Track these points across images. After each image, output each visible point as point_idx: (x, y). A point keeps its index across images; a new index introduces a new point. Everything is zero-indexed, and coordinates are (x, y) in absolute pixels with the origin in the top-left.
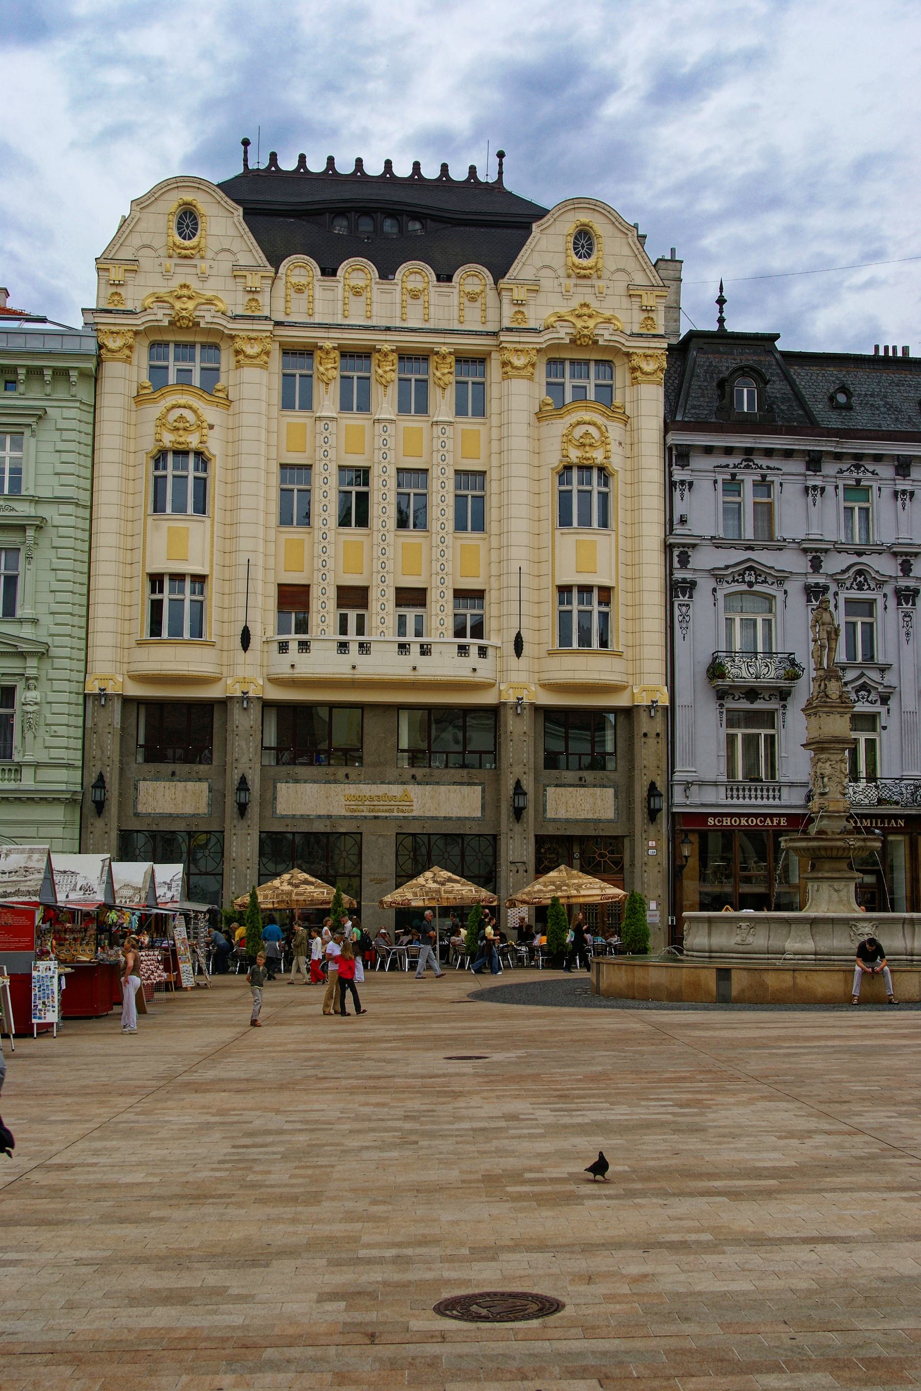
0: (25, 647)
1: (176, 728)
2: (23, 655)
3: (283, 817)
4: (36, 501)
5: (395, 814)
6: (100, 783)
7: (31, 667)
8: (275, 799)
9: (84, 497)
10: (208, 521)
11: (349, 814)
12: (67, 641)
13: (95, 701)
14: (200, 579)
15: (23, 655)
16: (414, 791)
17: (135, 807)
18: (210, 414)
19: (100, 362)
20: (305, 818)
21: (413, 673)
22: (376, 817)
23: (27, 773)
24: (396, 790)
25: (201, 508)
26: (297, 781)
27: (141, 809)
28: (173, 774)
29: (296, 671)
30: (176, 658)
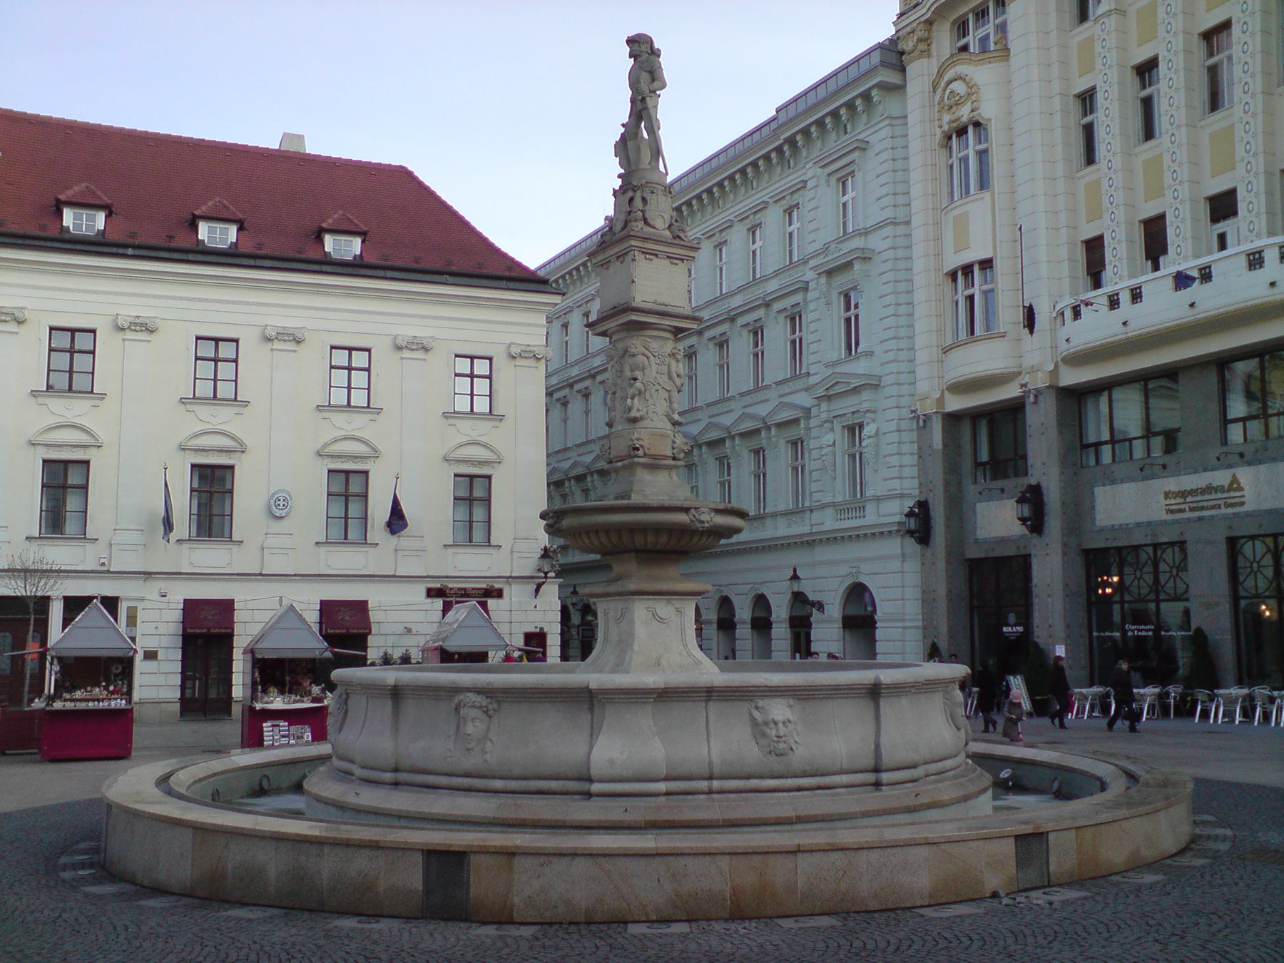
0: (855, 382)
1: (987, 436)
2: (856, 390)
3: (1102, 529)
4: (865, 233)
5: (1223, 510)
6: (921, 512)
7: (865, 400)
8: (1093, 508)
9: (901, 213)
10: (986, 195)
11: (1170, 517)
12: (893, 367)
13: (924, 422)
14: (987, 264)
15: (856, 390)
16: (1245, 475)
17: (975, 534)
18: (983, 74)
19: (903, 69)
20: (1125, 528)
21: (1191, 311)
22: (1200, 519)
23: (870, 507)
24: (1221, 477)
25: (984, 184)
26: (1113, 482)
27: (981, 534)
28: (1002, 491)
29: (1072, 344)
30: (983, 358)
